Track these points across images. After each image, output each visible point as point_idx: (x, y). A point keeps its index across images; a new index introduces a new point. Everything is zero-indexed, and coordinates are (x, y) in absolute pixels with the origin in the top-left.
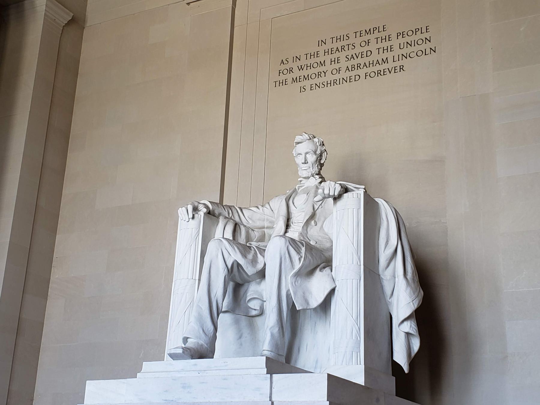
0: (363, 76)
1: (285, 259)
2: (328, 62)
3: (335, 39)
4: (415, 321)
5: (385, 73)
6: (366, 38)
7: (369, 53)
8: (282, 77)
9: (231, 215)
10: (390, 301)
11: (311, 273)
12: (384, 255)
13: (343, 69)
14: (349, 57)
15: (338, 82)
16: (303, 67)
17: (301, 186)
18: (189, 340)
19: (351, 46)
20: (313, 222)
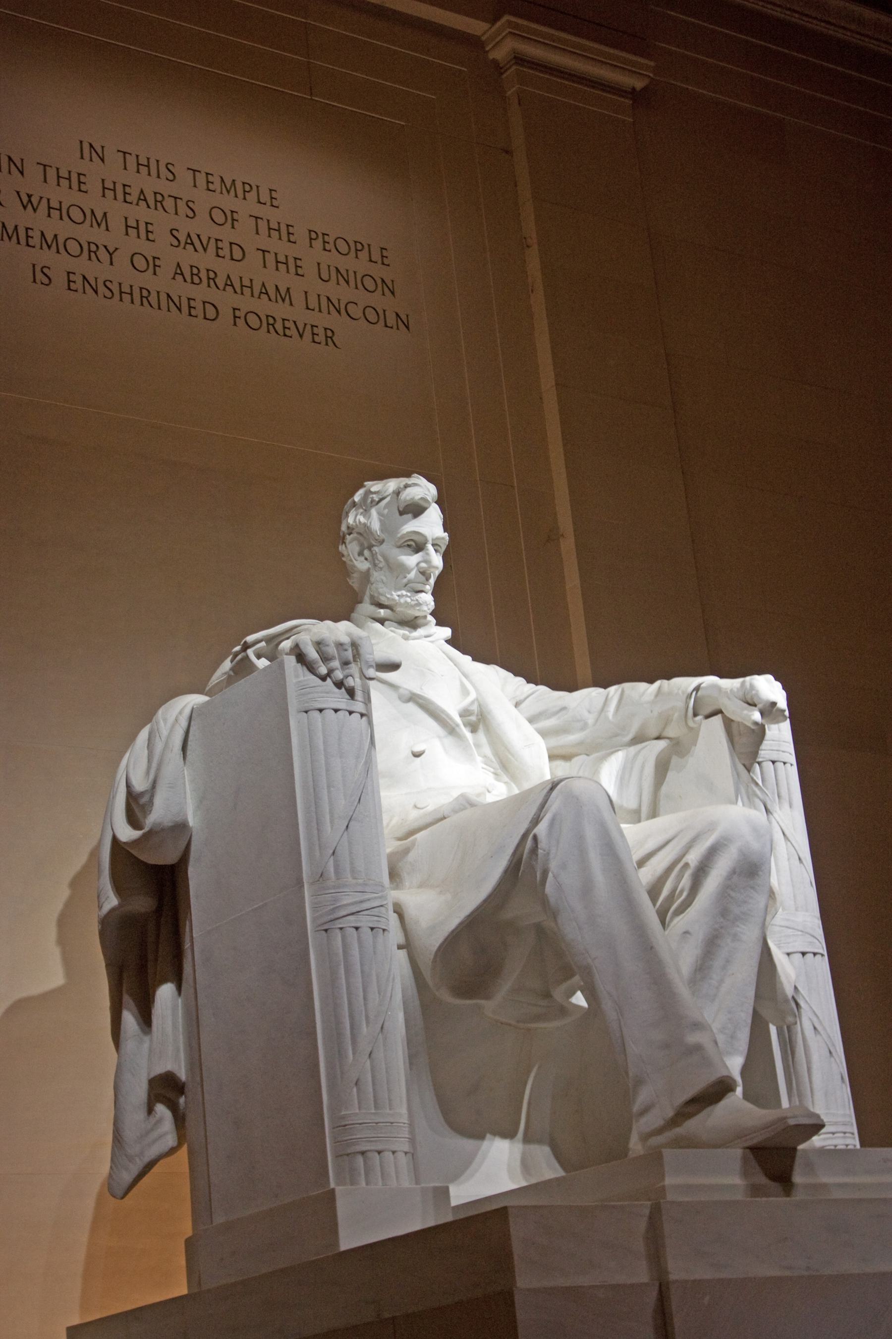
6: (228, 202)
7: (238, 254)
13: (167, 268)
14: (183, 239)
15: (153, 299)
16: (35, 200)
19: (181, 205)
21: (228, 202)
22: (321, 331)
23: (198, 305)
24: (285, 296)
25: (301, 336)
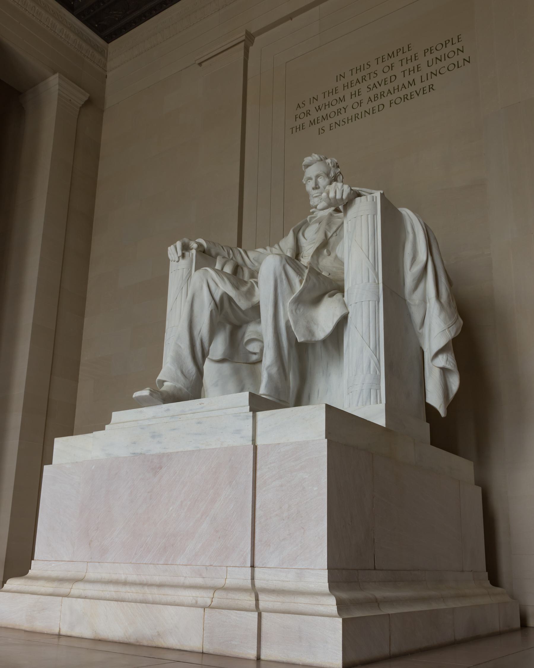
0: (387, 104)
1: (281, 281)
2: (348, 97)
3: (354, 71)
4: (453, 355)
5: (412, 97)
8: (299, 122)
9: (231, 256)
10: (420, 331)
11: (317, 301)
12: (410, 275)
14: (371, 87)
15: (359, 116)
16: (320, 107)
17: (315, 217)
18: (166, 384)
19: (372, 75)
20: (325, 251)
21: (389, 62)
22: (427, 88)
23: (377, 108)
24: (412, 83)
25: (418, 95)
